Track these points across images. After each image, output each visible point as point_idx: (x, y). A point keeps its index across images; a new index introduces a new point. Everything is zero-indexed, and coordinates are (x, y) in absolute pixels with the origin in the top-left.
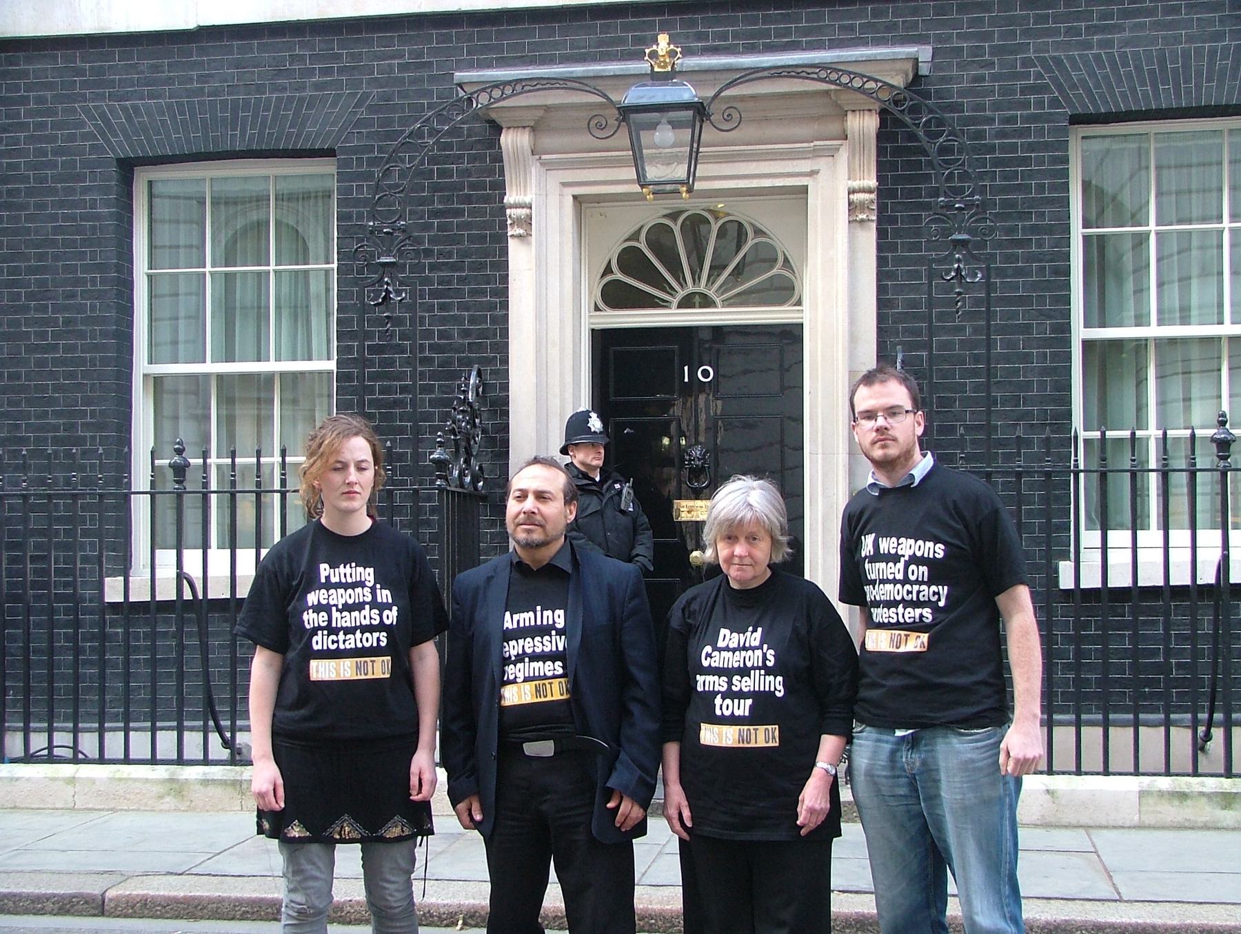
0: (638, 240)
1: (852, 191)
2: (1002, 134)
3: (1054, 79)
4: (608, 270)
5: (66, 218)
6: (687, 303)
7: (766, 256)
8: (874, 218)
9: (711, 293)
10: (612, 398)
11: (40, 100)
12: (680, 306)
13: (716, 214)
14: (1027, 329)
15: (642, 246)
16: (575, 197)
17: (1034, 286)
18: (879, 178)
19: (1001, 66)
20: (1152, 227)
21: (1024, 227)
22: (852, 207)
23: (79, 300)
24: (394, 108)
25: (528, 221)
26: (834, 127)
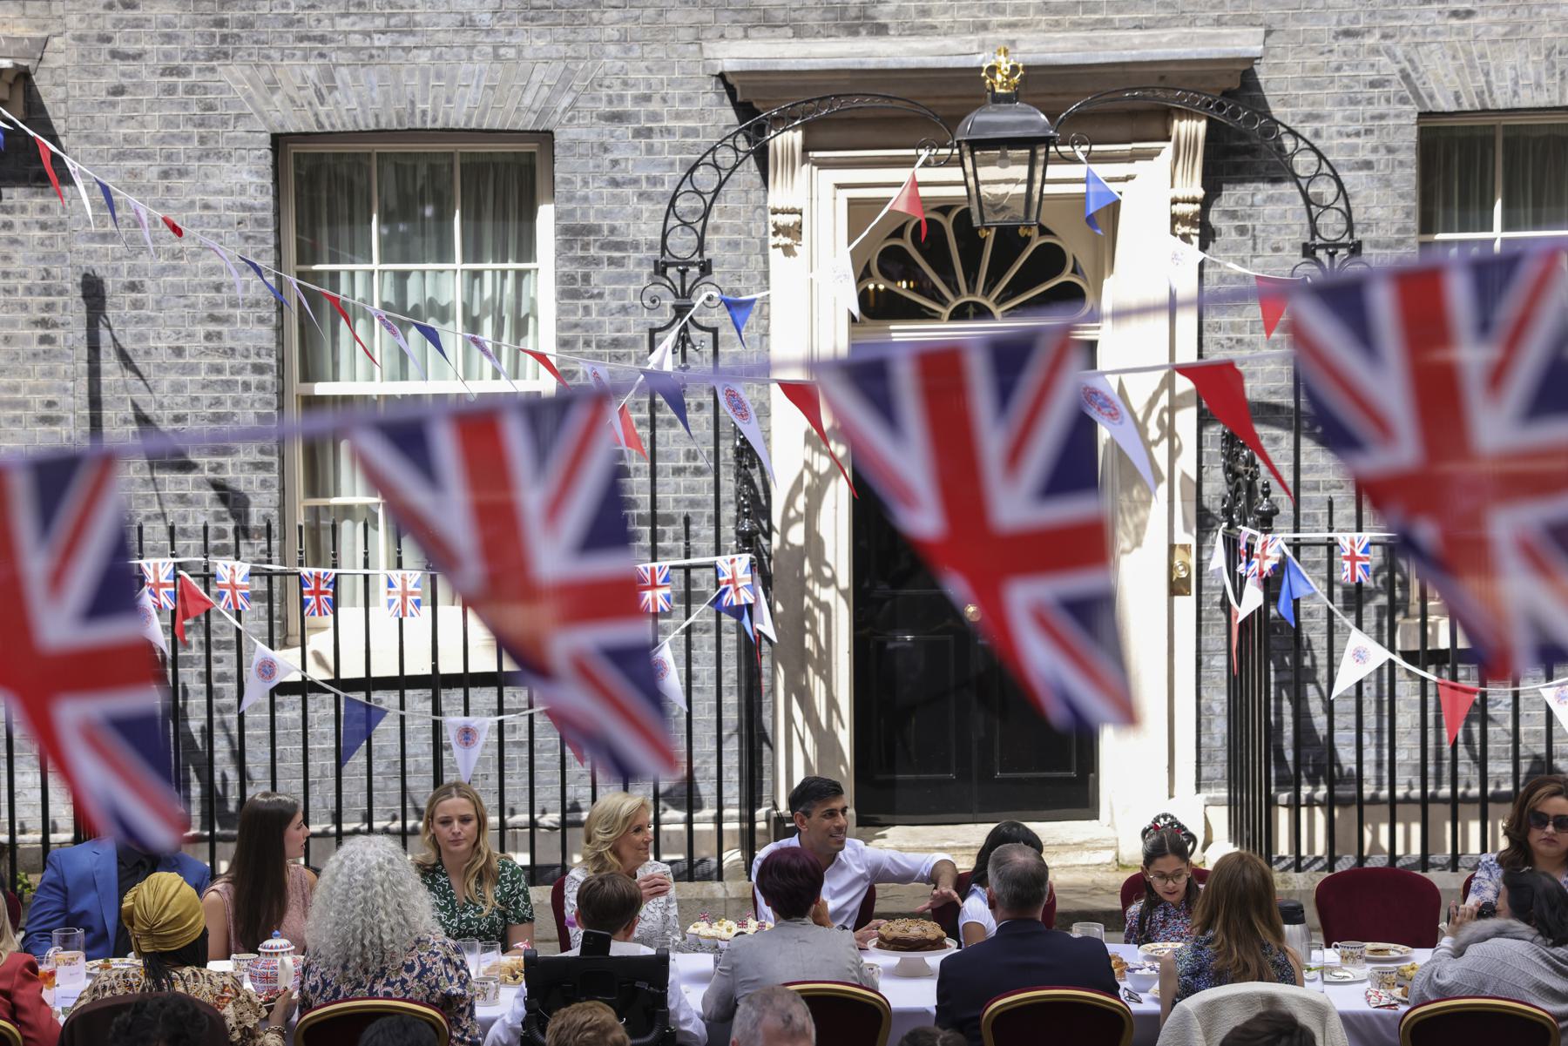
1: (1174, 202)
2: (1340, 134)
3: (1402, 71)
5: (206, 207)
6: (959, 314)
7: (1051, 259)
9: (989, 303)
11: (168, 56)
12: (952, 317)
15: (907, 243)
16: (852, 203)
18: (1204, 186)
19: (1345, 53)
22: (1175, 219)
23: (225, 311)
24: (625, 83)
25: (795, 231)
26: (1156, 127)
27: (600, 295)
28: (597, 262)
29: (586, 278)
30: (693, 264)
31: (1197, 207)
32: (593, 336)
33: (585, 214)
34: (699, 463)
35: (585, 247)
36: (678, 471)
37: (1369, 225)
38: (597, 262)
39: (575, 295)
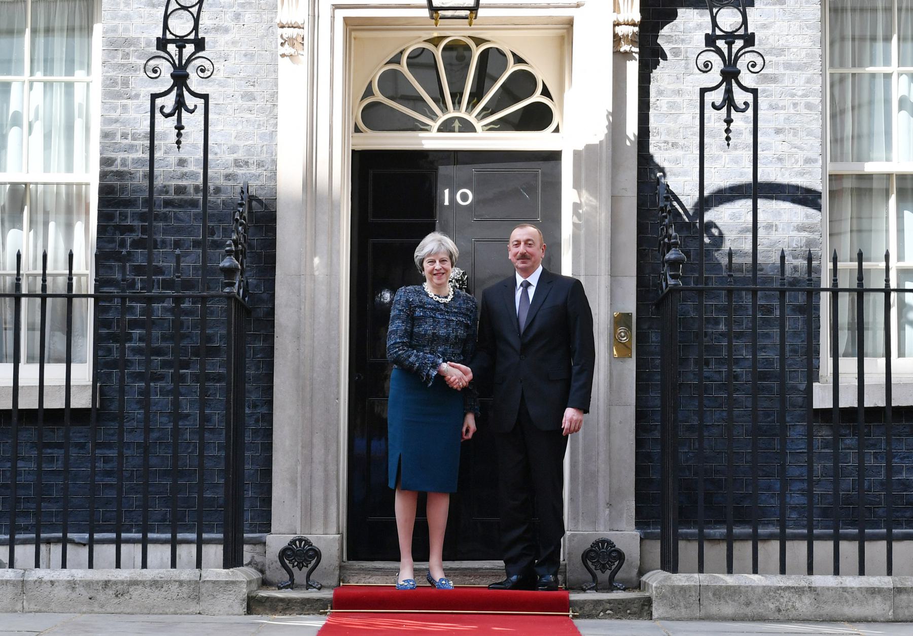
0: (399, 63)
1: (617, 24)
4: (369, 92)
6: (446, 127)
7: (524, 82)
8: (637, 50)
9: (471, 118)
10: (371, 219)
12: (439, 130)
13: (479, 41)
14: (780, 160)
16: (345, 19)
17: (787, 119)
18: (642, 11)
20: (894, 68)
21: (777, 64)
22: (617, 39)
27: (137, 96)
28: (134, 68)
29: (126, 83)
30: (190, 41)
31: (636, 29)
32: (128, 130)
33: (126, 30)
34: (215, 238)
35: (126, 56)
36: (196, 244)
37: (783, 50)
38: (134, 68)
39: (119, 96)
